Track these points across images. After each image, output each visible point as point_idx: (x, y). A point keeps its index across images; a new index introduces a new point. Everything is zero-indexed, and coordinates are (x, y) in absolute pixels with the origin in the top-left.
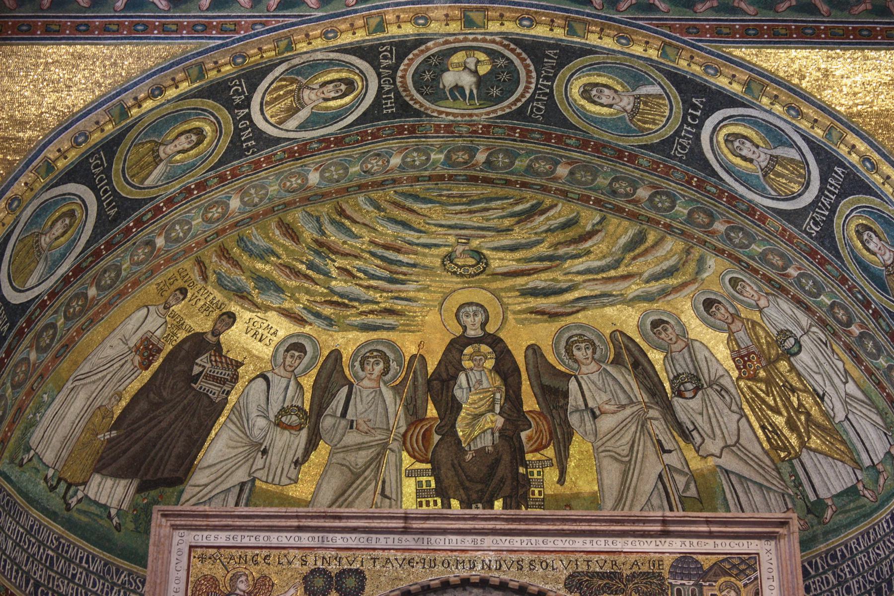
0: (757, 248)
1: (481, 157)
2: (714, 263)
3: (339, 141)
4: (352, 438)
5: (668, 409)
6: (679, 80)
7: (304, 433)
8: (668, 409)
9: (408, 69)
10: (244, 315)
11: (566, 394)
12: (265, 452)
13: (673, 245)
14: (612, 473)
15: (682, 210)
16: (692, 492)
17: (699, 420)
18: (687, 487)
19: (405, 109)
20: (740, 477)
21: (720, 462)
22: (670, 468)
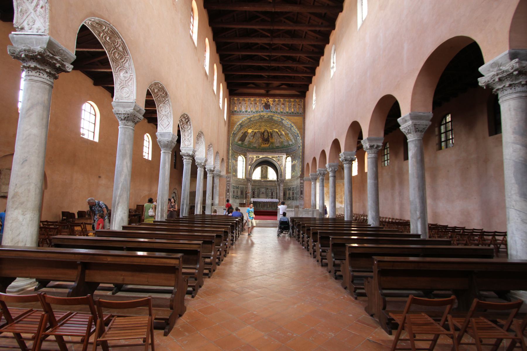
0: (286, 128)
1: (267, 120)
2: (283, 128)
3: (257, 120)
4: (256, 137)
5: (280, 136)
6: (281, 118)
7: (253, 137)
8: (280, 136)
9: (262, 116)
10: (249, 130)
11: (272, 135)
12: (250, 138)
13: (280, 127)
14: (275, 140)
15: (281, 125)
17: (282, 137)
19: (262, 118)
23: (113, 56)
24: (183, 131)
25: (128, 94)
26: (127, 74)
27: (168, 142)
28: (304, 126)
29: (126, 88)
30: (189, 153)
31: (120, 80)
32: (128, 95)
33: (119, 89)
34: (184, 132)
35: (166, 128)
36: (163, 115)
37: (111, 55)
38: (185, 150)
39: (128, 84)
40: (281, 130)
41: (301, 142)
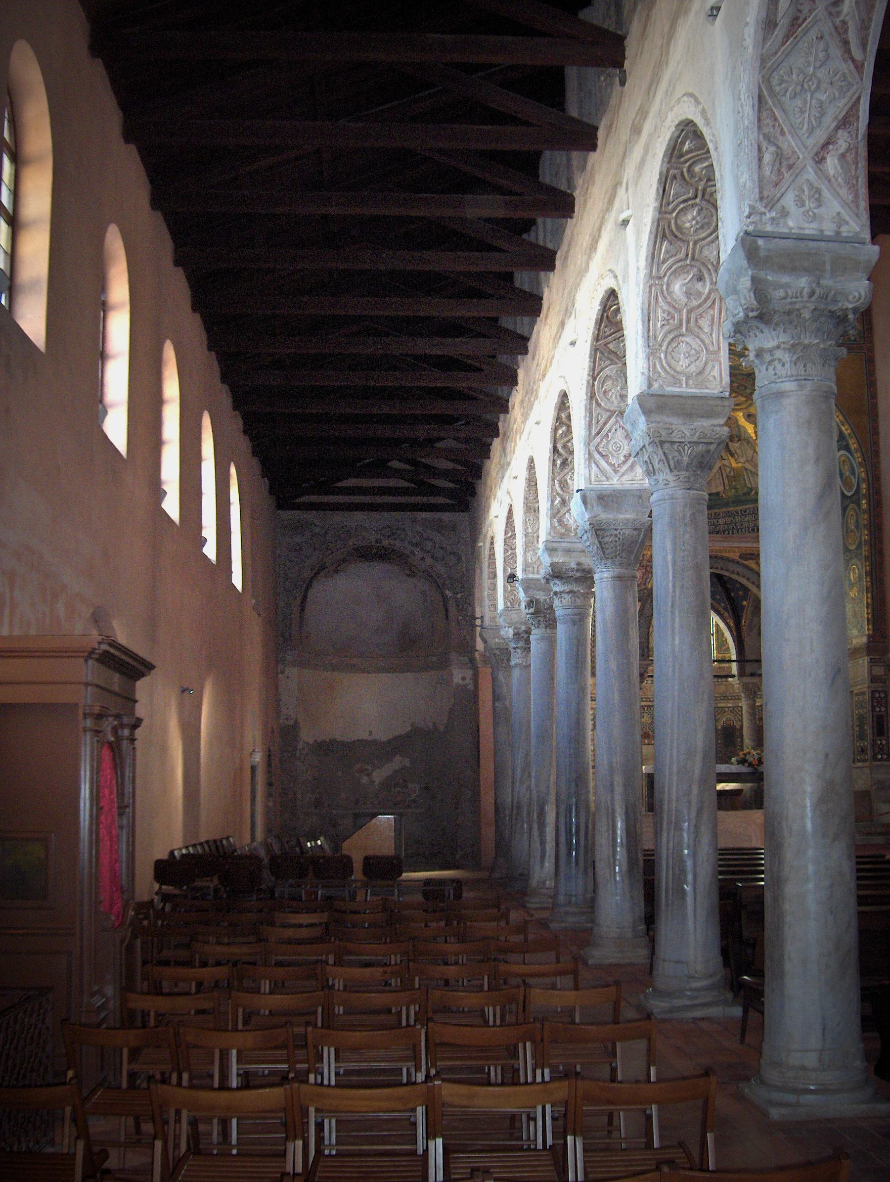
16: (732, 474)
17: (738, 451)
18: (730, 472)
20: (751, 472)
21: (744, 465)
22: (724, 465)
23: (673, 222)
24: (559, 462)
25: (697, 363)
26: (700, 284)
27: (635, 529)
28: (874, 396)
29: (688, 339)
30: (586, 567)
31: (666, 307)
32: (700, 364)
33: (663, 340)
34: (562, 470)
35: (625, 468)
36: (609, 413)
37: (669, 216)
38: (568, 551)
39: (696, 321)
40: (740, 415)
41: (863, 475)
